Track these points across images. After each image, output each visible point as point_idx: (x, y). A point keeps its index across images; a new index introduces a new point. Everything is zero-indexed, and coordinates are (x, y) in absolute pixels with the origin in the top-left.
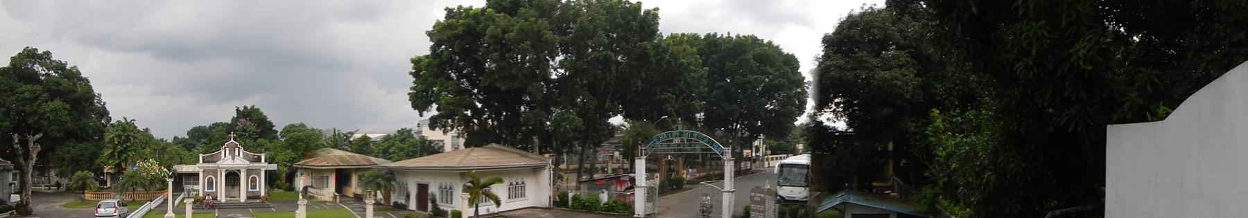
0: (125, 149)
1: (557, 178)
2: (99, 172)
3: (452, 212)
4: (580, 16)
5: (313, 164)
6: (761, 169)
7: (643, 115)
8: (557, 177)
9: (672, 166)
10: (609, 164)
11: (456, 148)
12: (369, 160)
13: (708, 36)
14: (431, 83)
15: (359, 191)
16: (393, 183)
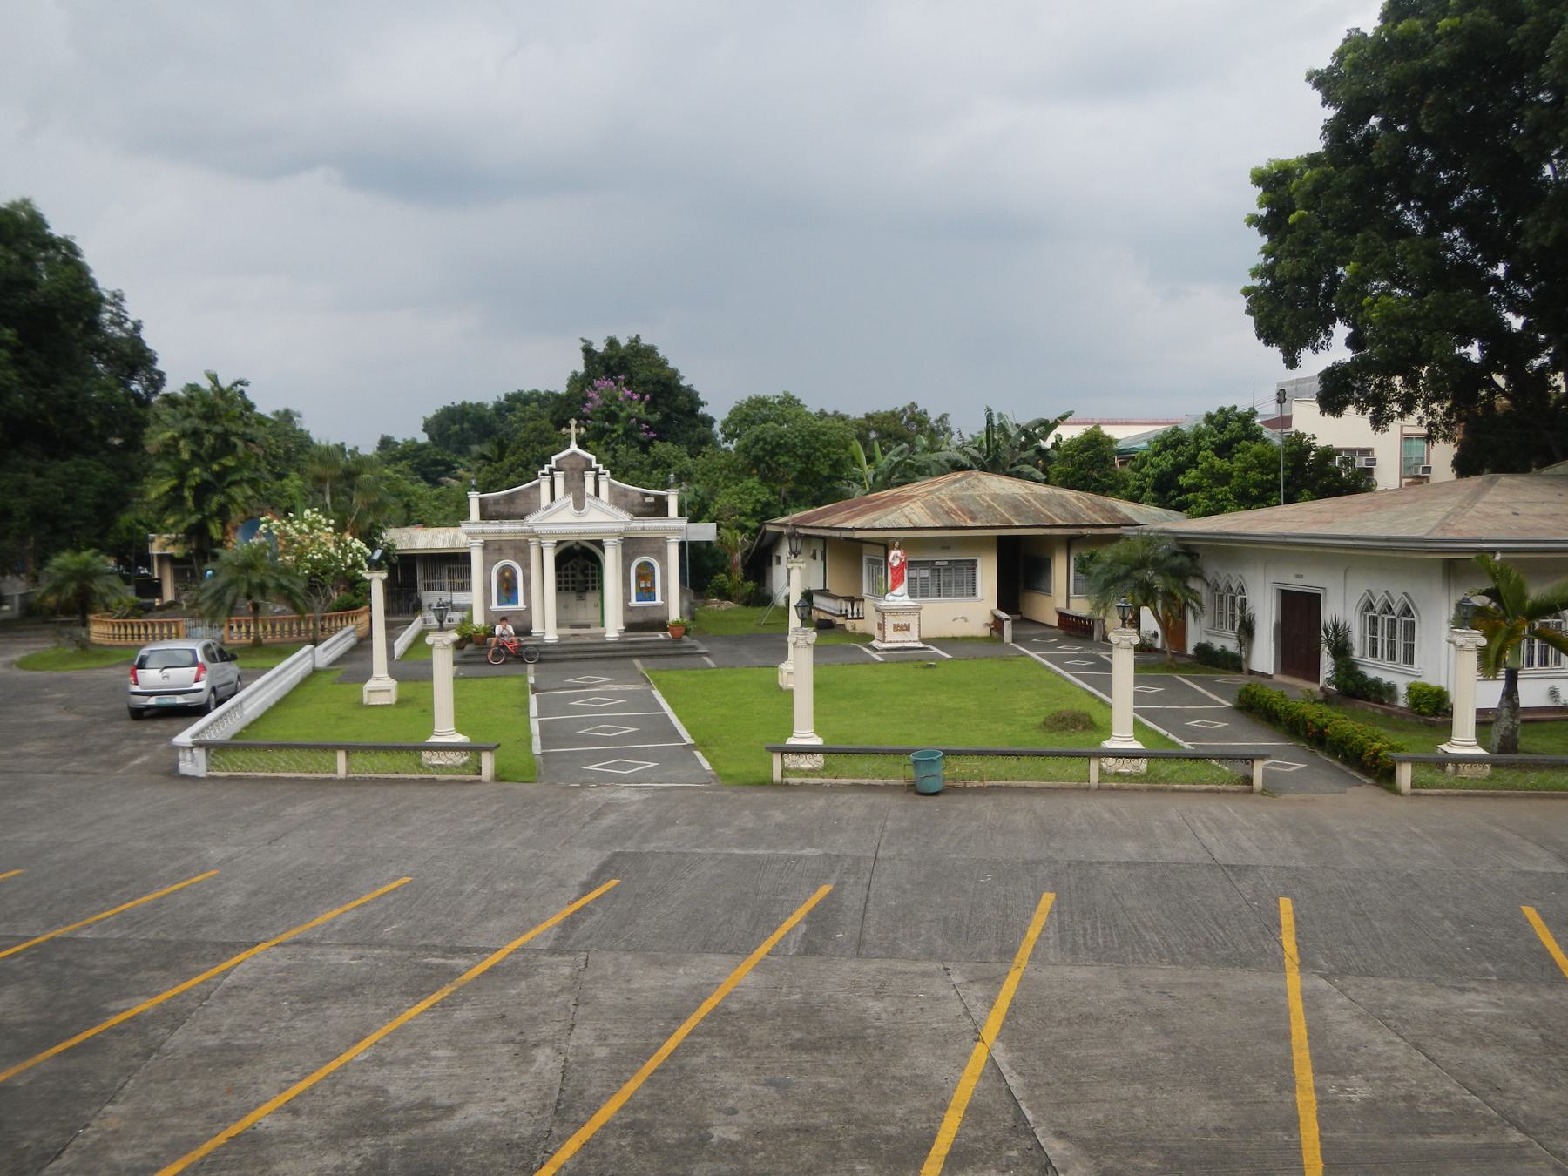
0: (220, 476)
2: (132, 555)
3: (1410, 689)
5: (828, 522)
11: (1418, 476)
12: (1113, 510)
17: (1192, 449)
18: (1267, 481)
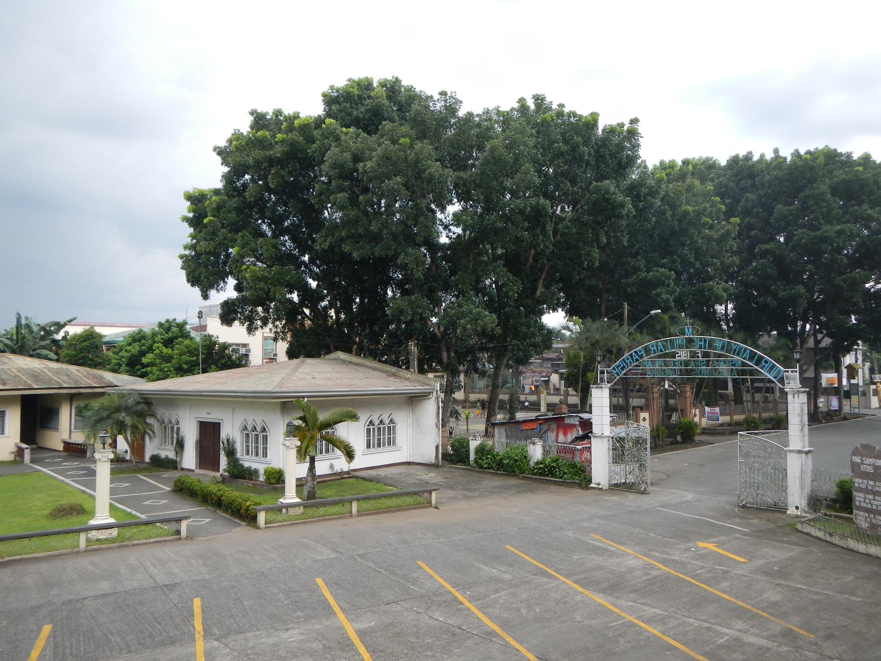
1: (449, 414)
4: (491, 138)
6: (863, 411)
7: (603, 310)
8: (449, 412)
9: (671, 402)
11: (272, 359)
12: (101, 377)
14: (225, 239)
15: (78, 438)
16: (150, 420)
17: (150, 342)
18: (193, 361)
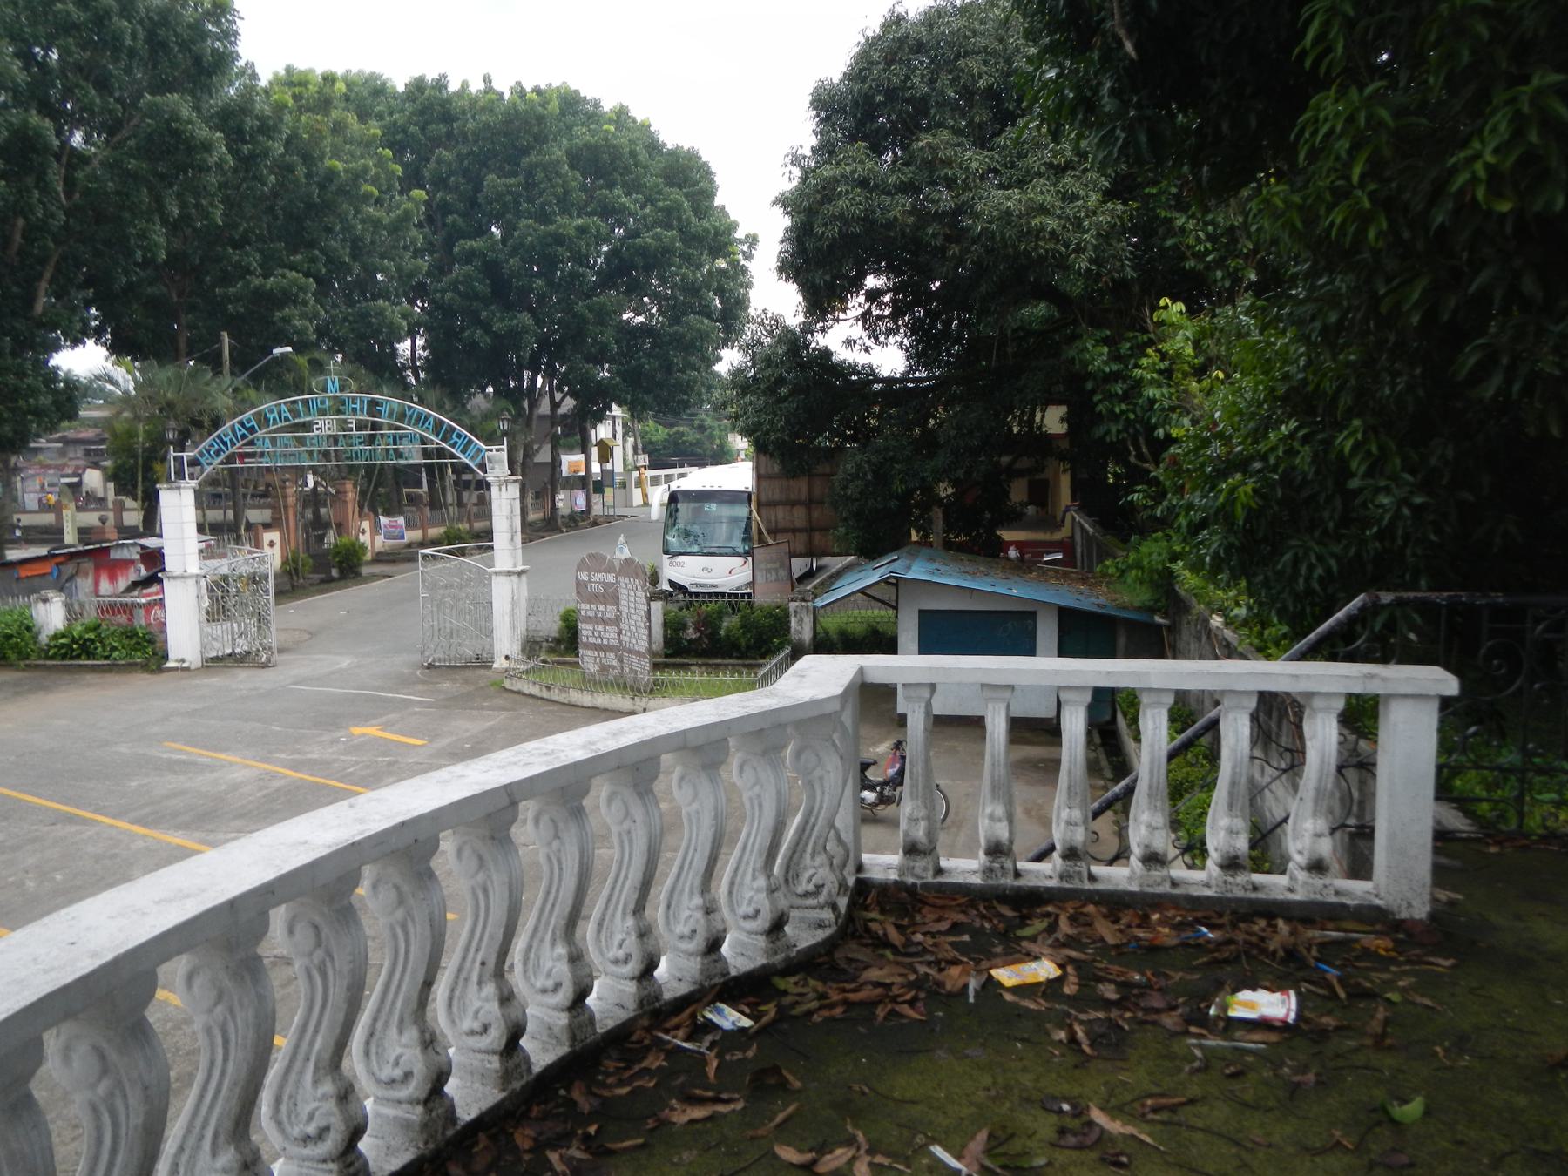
7: (182, 345)
10: (67, 514)
13: (418, 86)
